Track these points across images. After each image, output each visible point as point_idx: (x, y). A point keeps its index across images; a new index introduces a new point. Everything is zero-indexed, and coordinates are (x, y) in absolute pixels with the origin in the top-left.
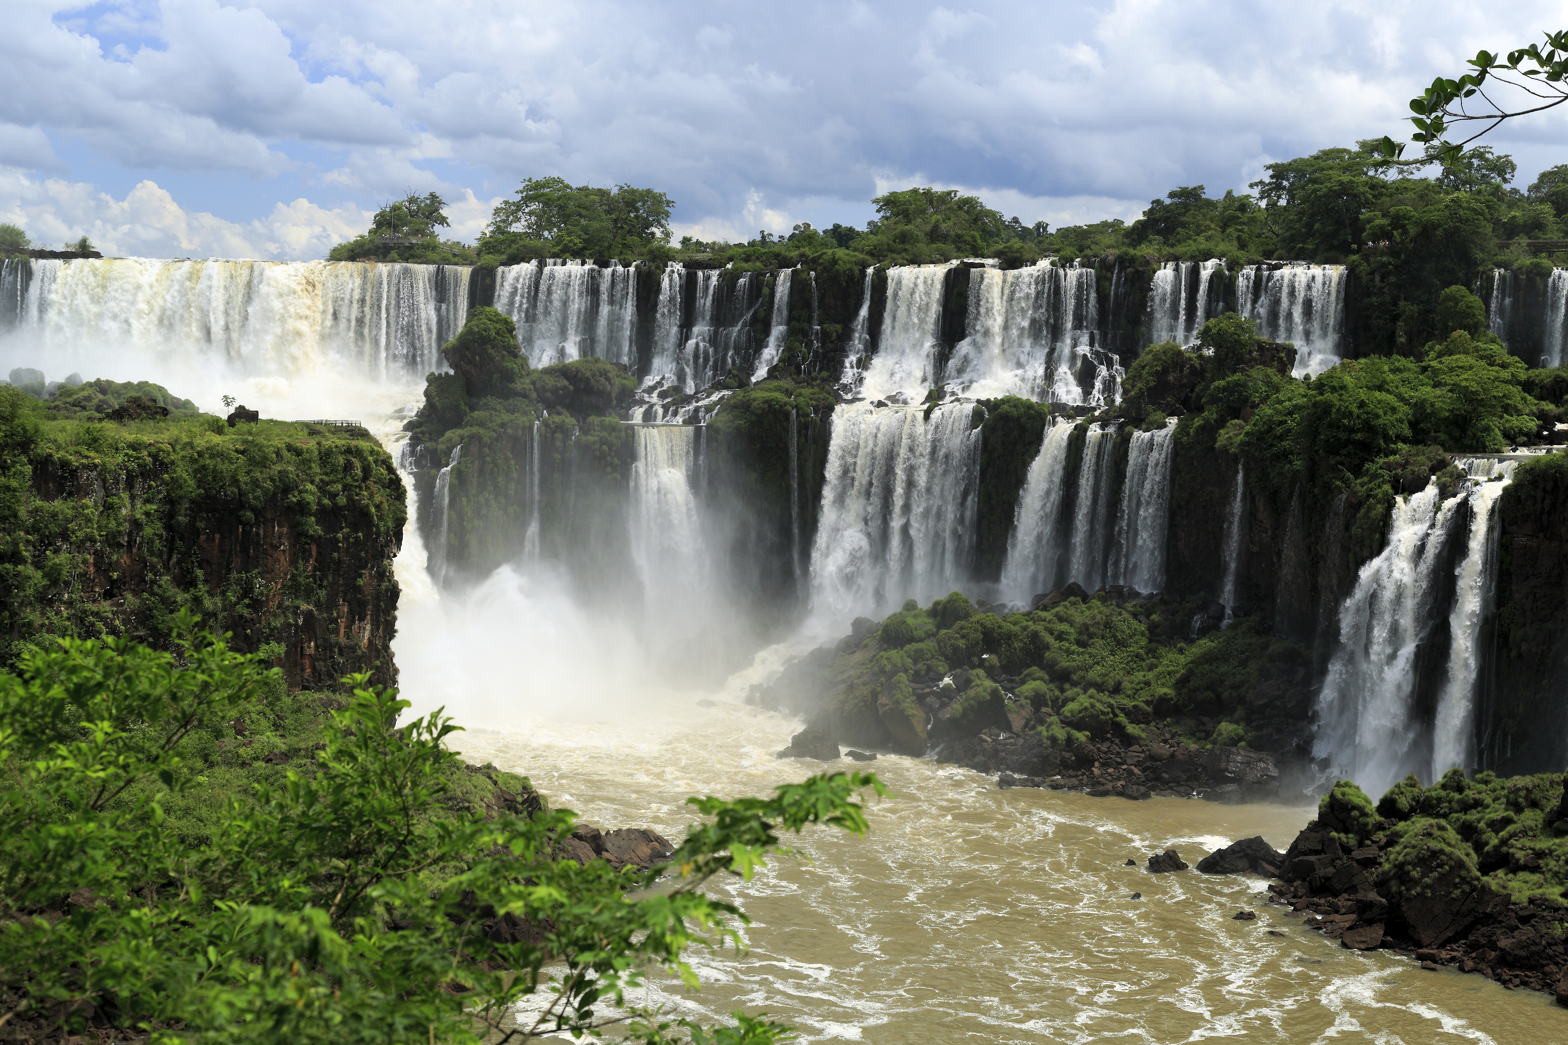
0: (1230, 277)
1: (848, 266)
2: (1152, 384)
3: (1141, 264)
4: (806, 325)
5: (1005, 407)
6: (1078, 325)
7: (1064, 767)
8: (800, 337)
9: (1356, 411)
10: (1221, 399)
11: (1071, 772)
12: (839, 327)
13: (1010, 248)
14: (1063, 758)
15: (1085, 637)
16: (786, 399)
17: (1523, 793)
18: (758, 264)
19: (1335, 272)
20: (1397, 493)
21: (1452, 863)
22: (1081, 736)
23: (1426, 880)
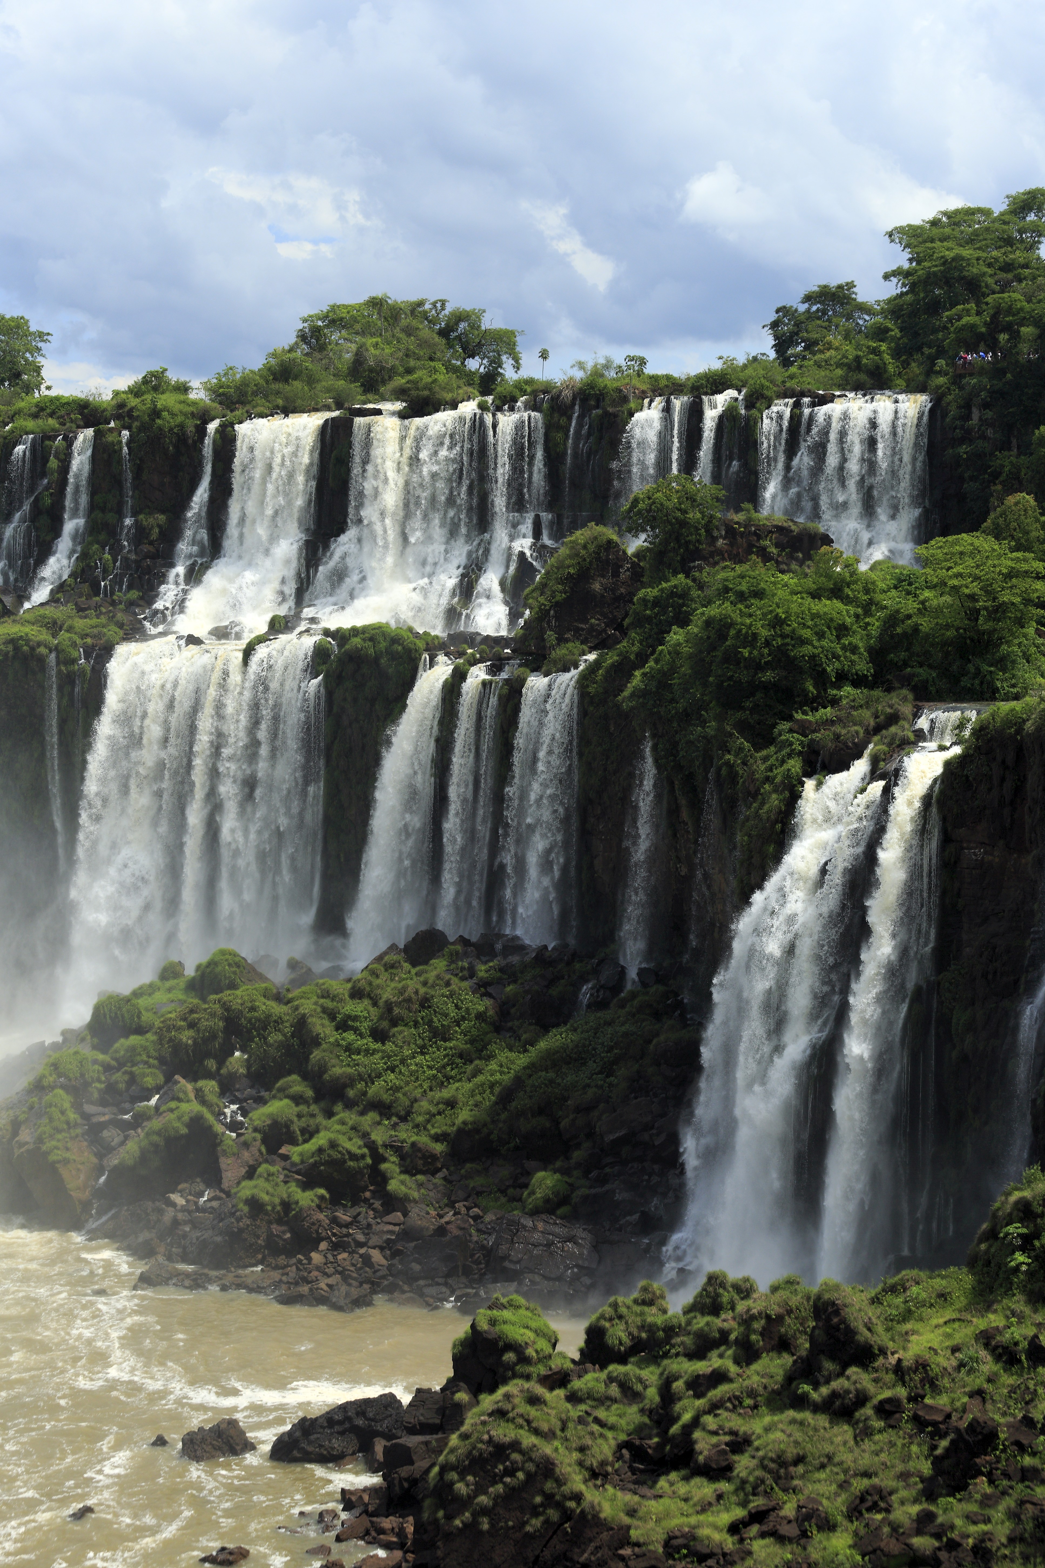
0: (748, 419)
1: (180, 419)
2: (559, 597)
3: (614, 403)
4: (111, 517)
5: (356, 641)
6: (518, 504)
7: (273, 1250)
8: (103, 537)
9: (764, 633)
10: (649, 619)
11: (282, 1260)
12: (162, 518)
13: (415, 382)
14: (270, 1235)
15: (385, 1024)
16: (45, 636)
17: (758, 1325)
18: (51, 422)
19: (912, 406)
20: (809, 775)
21: (531, 1467)
22: (306, 1198)
23: (483, 1499)
